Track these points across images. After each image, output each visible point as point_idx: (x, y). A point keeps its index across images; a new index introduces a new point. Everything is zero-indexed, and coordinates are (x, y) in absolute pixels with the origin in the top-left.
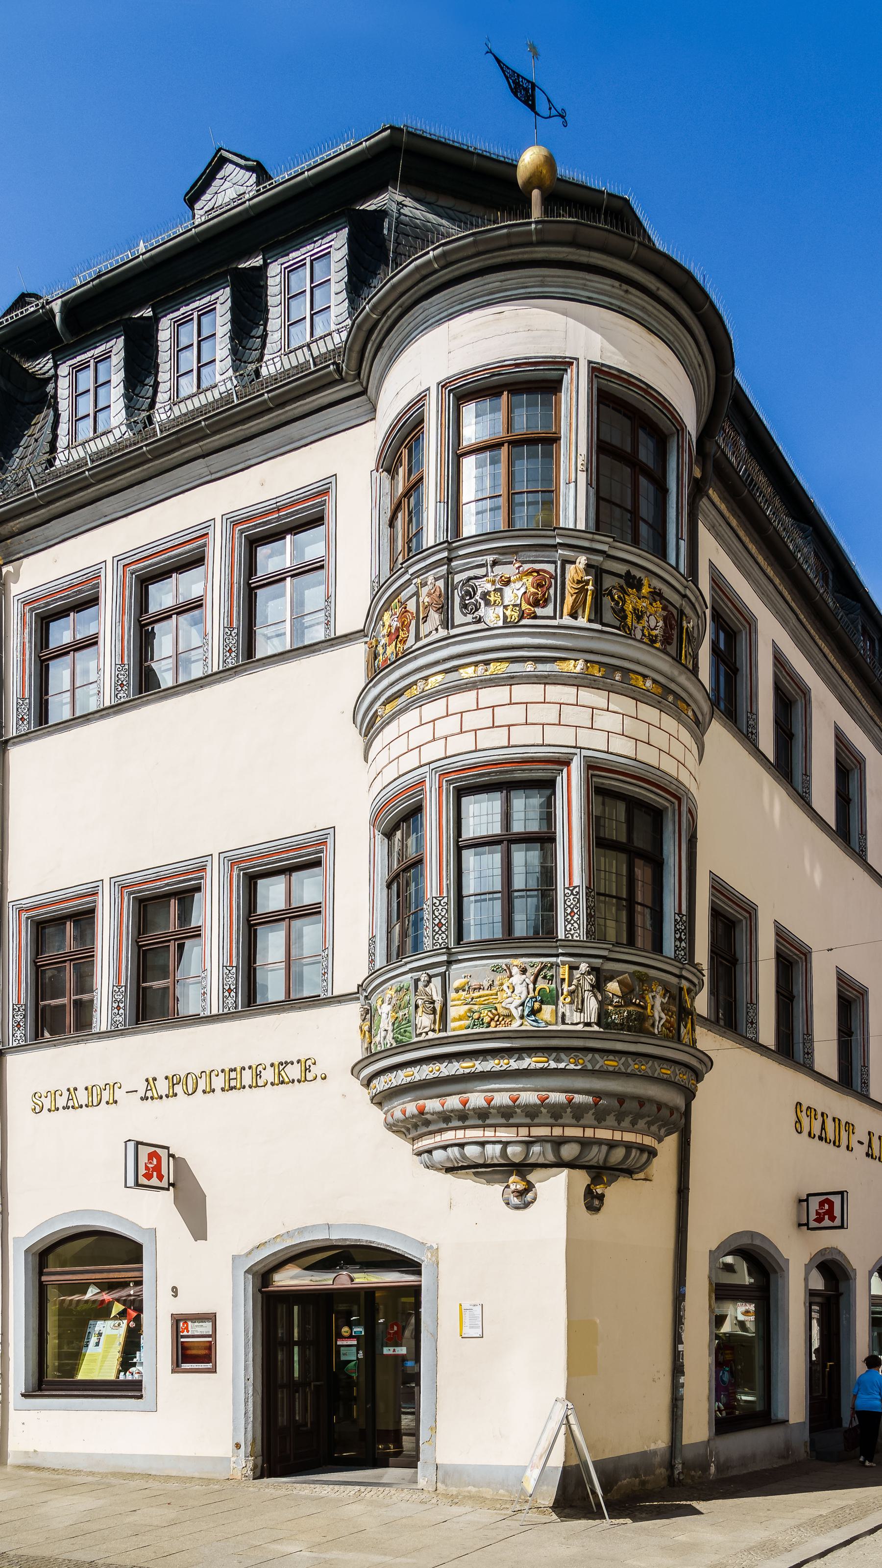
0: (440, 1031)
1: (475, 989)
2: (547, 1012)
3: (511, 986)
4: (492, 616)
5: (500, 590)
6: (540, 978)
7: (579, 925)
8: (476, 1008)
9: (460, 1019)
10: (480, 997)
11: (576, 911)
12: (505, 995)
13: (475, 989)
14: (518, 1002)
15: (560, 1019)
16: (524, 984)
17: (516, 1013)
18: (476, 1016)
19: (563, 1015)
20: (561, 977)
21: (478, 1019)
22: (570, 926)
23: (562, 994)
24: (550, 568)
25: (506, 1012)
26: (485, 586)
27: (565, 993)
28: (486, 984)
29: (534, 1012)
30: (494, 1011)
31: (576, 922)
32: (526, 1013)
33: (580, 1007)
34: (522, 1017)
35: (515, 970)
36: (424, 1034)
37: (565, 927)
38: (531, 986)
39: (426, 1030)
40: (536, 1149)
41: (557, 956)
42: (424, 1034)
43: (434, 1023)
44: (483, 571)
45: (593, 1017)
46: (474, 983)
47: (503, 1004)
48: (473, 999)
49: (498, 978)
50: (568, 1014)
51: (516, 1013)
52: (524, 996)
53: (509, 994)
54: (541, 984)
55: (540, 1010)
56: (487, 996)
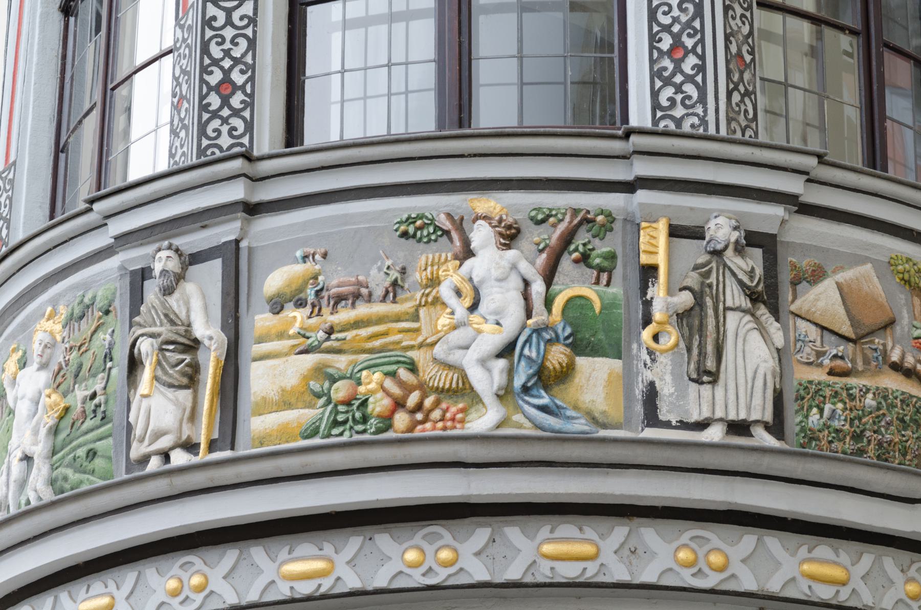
0: (212, 446)
1: (339, 299)
3: (467, 289)
6: (566, 264)
7: (702, 90)
9: (285, 403)
10: (357, 324)
11: (689, 43)
12: (444, 321)
13: (339, 299)
15: (639, 409)
16: (515, 283)
17: (486, 380)
18: (340, 390)
19: (651, 395)
20: (645, 259)
21: (348, 403)
22: (669, 92)
23: (647, 320)
25: (444, 379)
27: (658, 314)
28: (378, 282)
30: (403, 374)
31: (690, 79)
32: (518, 382)
33: (710, 364)
34: (504, 395)
37: (655, 94)
38: (538, 287)
39: (164, 443)
41: (629, 187)
45: (757, 401)
46: (336, 279)
48: (330, 332)
50: (666, 389)
51: (486, 380)
54: (574, 284)
55: (566, 374)
56: (380, 320)
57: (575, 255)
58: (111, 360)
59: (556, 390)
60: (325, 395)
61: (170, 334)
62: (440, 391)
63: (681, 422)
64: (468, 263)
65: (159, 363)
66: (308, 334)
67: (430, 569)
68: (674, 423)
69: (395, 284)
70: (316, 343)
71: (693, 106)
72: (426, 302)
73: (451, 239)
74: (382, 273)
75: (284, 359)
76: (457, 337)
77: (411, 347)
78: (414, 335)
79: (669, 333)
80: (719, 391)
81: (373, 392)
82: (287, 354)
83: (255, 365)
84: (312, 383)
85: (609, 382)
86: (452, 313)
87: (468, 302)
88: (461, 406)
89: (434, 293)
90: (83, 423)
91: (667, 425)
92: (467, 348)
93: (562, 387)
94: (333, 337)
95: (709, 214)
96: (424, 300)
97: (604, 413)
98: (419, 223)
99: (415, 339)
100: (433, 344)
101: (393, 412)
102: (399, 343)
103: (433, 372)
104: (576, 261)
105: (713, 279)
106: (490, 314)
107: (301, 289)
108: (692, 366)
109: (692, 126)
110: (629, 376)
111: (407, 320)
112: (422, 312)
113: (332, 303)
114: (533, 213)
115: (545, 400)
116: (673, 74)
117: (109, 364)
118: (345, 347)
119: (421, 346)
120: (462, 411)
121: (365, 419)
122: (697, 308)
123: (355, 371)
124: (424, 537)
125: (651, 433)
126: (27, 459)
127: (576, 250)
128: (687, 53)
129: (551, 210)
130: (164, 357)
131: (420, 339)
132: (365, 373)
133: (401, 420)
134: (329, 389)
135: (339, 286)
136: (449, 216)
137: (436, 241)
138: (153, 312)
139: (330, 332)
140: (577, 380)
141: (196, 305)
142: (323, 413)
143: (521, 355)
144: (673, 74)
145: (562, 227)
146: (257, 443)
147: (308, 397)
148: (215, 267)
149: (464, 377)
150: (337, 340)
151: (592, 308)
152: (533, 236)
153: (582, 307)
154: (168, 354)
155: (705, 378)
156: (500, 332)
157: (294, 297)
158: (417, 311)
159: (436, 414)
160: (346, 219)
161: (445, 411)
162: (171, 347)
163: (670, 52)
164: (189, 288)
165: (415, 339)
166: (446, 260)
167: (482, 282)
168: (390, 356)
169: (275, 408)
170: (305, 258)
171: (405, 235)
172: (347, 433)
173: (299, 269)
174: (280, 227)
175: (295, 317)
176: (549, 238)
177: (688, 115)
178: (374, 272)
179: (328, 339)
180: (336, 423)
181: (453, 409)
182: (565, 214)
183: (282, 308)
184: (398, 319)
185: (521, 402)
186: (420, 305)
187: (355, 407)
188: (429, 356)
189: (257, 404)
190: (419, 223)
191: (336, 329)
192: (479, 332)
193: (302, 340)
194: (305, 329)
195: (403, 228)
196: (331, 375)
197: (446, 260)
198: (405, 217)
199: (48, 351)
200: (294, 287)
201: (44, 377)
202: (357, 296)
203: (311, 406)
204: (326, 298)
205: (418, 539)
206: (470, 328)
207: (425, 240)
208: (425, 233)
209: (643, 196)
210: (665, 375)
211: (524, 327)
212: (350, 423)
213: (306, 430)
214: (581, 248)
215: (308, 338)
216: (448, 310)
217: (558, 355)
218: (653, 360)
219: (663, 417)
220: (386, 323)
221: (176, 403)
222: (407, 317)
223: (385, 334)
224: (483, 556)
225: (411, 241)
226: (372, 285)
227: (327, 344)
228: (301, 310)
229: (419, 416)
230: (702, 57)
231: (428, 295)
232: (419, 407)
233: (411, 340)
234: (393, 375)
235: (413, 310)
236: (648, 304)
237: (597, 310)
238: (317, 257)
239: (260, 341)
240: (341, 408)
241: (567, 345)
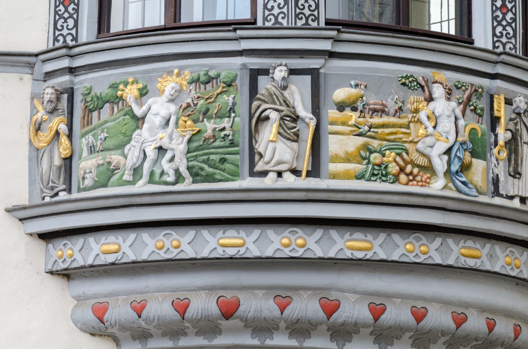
0: (309, 174)
1: (375, 111)
6: (468, 111)
7: (515, 31)
8: (375, 144)
9: (347, 159)
10: (383, 126)
12: (421, 131)
14: (443, 146)
17: (440, 164)
18: (375, 158)
20: (496, 114)
21: (379, 165)
22: (499, 29)
23: (496, 144)
25: (422, 161)
27: (501, 142)
30: (404, 154)
31: (509, 24)
34: (448, 173)
35: (438, 91)
36: (272, 176)
37: (494, 29)
42: (272, 176)
43: (298, 157)
46: (372, 100)
47: (420, 146)
49: (414, 98)
50: (502, 179)
51: (440, 164)
52: (452, 138)
53: (430, 130)
56: (394, 126)
57: (472, 107)
58: (234, 112)
59: (465, 173)
60: (367, 159)
61: (289, 112)
62: (418, 166)
63: (506, 195)
64: (432, 104)
65: (280, 125)
66: (359, 126)
67: (417, 254)
68: (504, 196)
69: (400, 108)
70: (364, 132)
71: (510, 38)
72: (414, 121)
73: (424, 90)
74: (393, 102)
75: (348, 137)
76: (429, 141)
77: (406, 142)
78: (407, 136)
79: (503, 151)
80: (521, 181)
81: (390, 162)
82: (348, 134)
83: (330, 136)
84: (362, 152)
85: (483, 172)
86: (426, 128)
87: (433, 124)
88: (429, 175)
89: (417, 117)
90: (213, 142)
91: (501, 196)
92: (432, 147)
93: (467, 172)
94: (372, 130)
95: (516, 94)
96: (413, 119)
97: (481, 187)
98: (411, 79)
99: (408, 138)
100: (416, 143)
101: (399, 174)
102: (401, 139)
103: (417, 157)
104: (472, 110)
105: (518, 127)
106: (444, 133)
107: (355, 102)
108: (511, 169)
109: (510, 48)
110: (488, 169)
111: (404, 128)
112: (412, 125)
113: (371, 112)
114: (457, 84)
115: (464, 179)
116: (502, 20)
117: (233, 115)
118: (377, 136)
119: (411, 142)
120: (429, 178)
121: (386, 175)
122: (513, 140)
123: (383, 149)
124: (414, 238)
125: (497, 201)
126: (161, 150)
127: (473, 105)
128: (508, 10)
129: (463, 83)
130: (284, 123)
131: (411, 139)
132: (387, 152)
133: (403, 178)
134: (369, 156)
135: (374, 105)
136: (423, 78)
137: (416, 90)
138: (274, 97)
139: (370, 127)
140: (472, 170)
141: (297, 97)
142: (367, 168)
143: (456, 155)
144: (502, 20)
145: (468, 93)
146: (332, 177)
147: (359, 159)
148: (307, 79)
149: (430, 161)
150: (374, 132)
151: (478, 135)
152: (457, 94)
153: (474, 133)
154: (286, 122)
155: (517, 176)
156: (448, 142)
157: (351, 105)
158: (409, 124)
159: (419, 178)
160: (377, 70)
161: (422, 177)
162: (288, 119)
163: (500, 9)
164: (293, 87)
165: (408, 138)
166: (422, 101)
167: (440, 116)
168: (398, 145)
169: (342, 161)
170: (357, 86)
171: (404, 84)
172: (378, 180)
173: (354, 91)
174: (342, 67)
175: (351, 116)
176: (463, 97)
177: (508, 42)
178: (389, 100)
179: (369, 131)
180: (374, 175)
181: (425, 176)
182: (468, 86)
183: (344, 110)
184: (401, 127)
185: (454, 178)
186: (411, 122)
187: (383, 168)
188: (414, 148)
189: (332, 157)
190: (411, 79)
191: (373, 126)
192: (438, 140)
193: (356, 128)
194: (357, 123)
195: (404, 80)
196: (371, 149)
197: (422, 101)
198: (405, 75)
199: (176, 93)
200: (351, 100)
201: (173, 108)
202: (383, 111)
203: (360, 163)
204: (368, 109)
205: (411, 239)
206: (434, 138)
207: (413, 88)
208: (413, 85)
209: (499, 83)
210: (501, 171)
211: (456, 141)
212: (380, 175)
213: (359, 175)
214: (474, 104)
215: (360, 128)
216: (423, 127)
217: (467, 157)
218: (498, 164)
219: (502, 192)
220: (396, 128)
221: (292, 149)
222: (405, 126)
223: (395, 133)
224: (438, 251)
225: (406, 88)
226: (389, 106)
227: (369, 133)
228: (355, 113)
229: (411, 178)
230: (515, 14)
231: (415, 117)
232: (411, 173)
233: (406, 138)
234: (399, 155)
235: (407, 123)
236: (496, 136)
237: (480, 136)
238: (362, 86)
239: (332, 123)
240: (376, 167)
241: (469, 152)
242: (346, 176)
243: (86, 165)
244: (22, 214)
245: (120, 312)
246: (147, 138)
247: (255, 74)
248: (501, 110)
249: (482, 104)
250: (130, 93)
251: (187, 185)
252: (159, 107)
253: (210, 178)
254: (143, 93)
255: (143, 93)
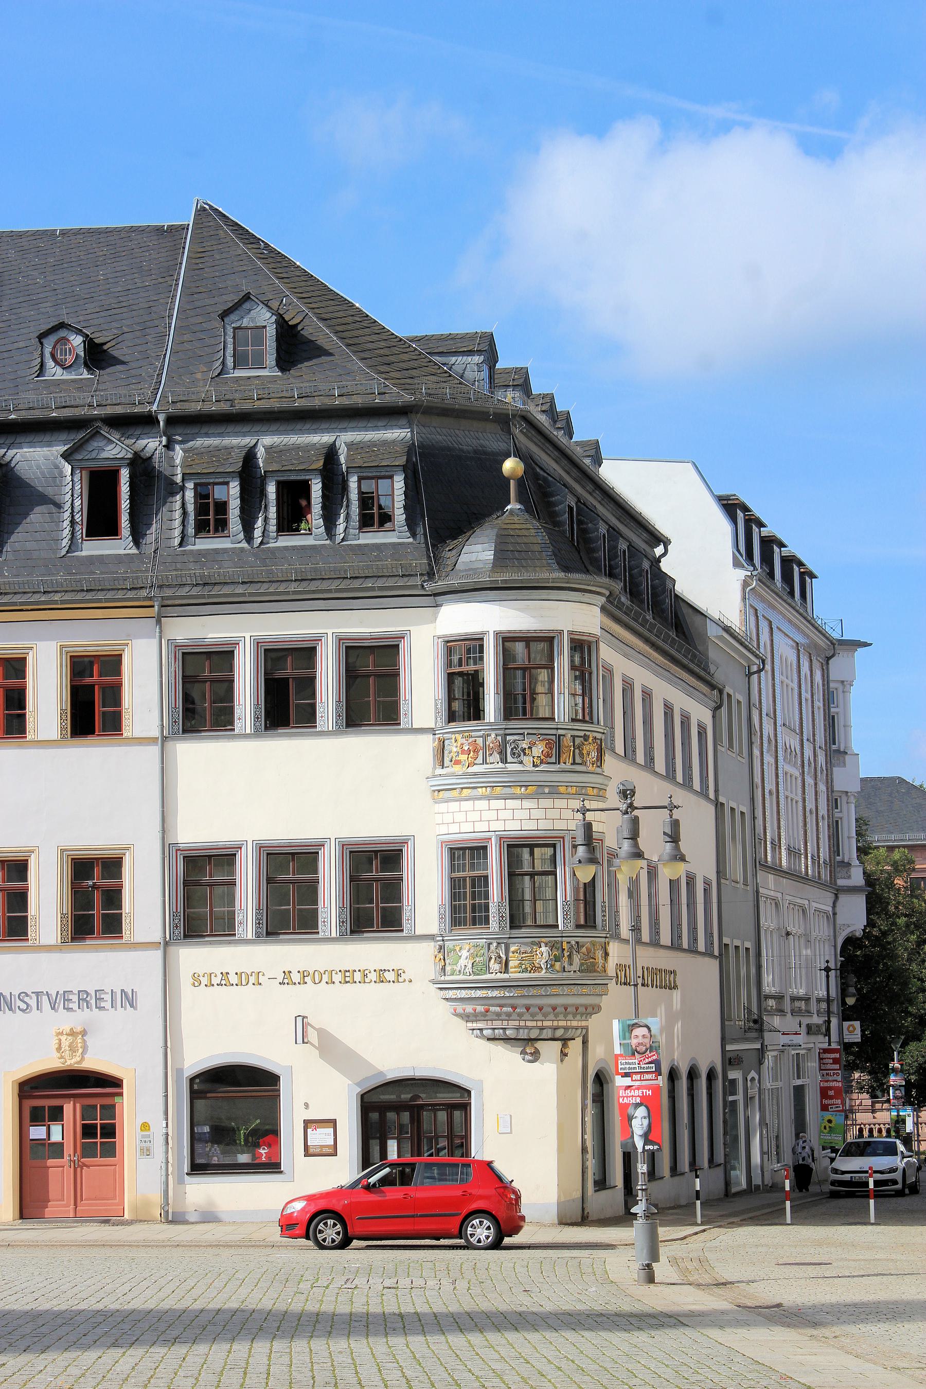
2: (558, 965)
4: (527, 760)
5: (530, 748)
18: (523, 966)
24: (553, 738)
26: (525, 745)
29: (552, 966)
35: (543, 945)
40: (545, 1031)
44: (520, 737)
242: (515, 972)
243: (448, 968)
244: (434, 982)
245: (460, 1010)
246: (462, 962)
247: (489, 944)
248: (565, 946)
249: (559, 945)
250: (458, 949)
251: (472, 977)
252: (465, 953)
253: (478, 975)
254: (461, 949)
255: (461, 949)
